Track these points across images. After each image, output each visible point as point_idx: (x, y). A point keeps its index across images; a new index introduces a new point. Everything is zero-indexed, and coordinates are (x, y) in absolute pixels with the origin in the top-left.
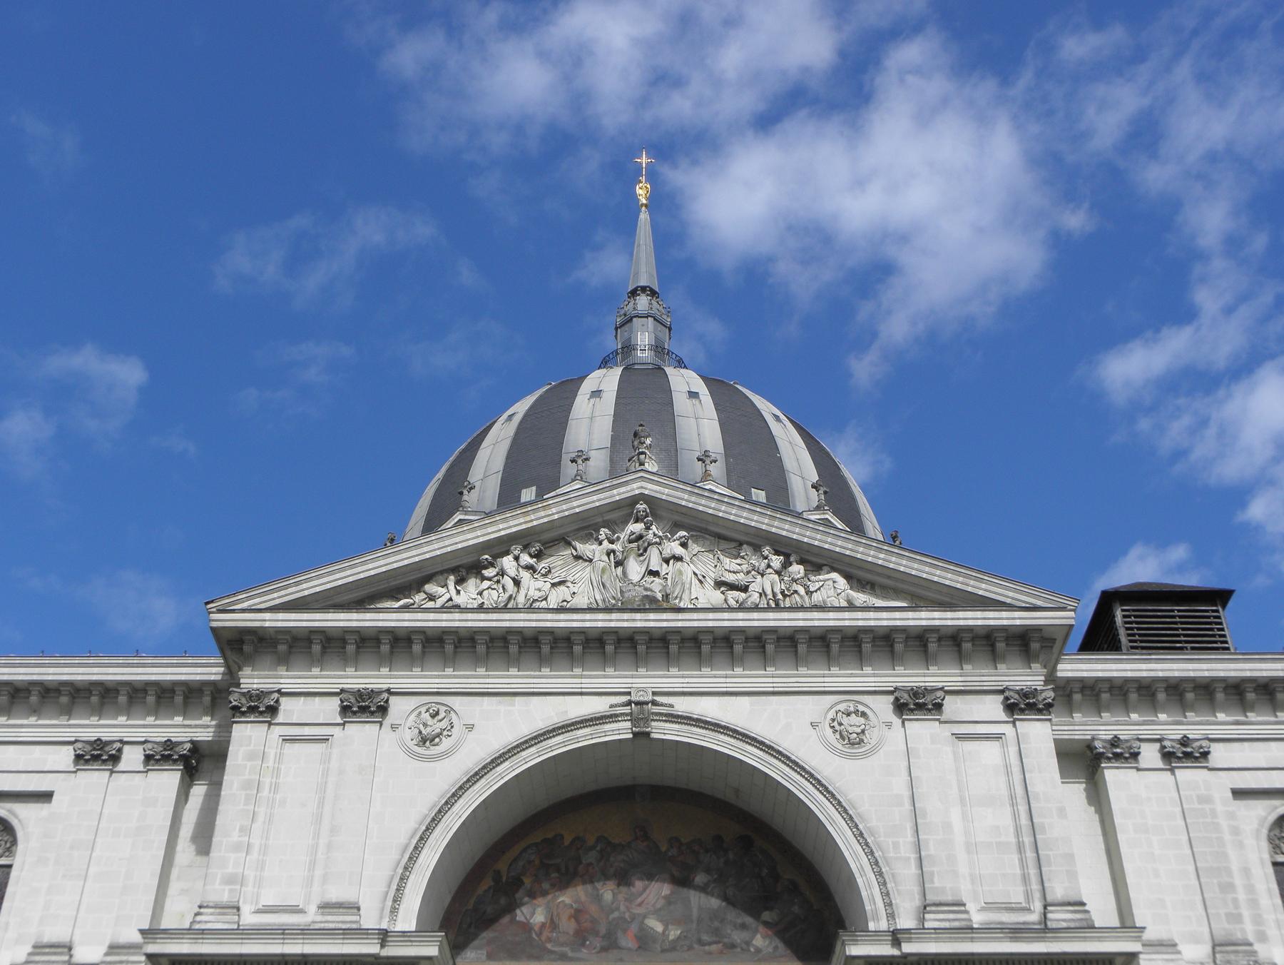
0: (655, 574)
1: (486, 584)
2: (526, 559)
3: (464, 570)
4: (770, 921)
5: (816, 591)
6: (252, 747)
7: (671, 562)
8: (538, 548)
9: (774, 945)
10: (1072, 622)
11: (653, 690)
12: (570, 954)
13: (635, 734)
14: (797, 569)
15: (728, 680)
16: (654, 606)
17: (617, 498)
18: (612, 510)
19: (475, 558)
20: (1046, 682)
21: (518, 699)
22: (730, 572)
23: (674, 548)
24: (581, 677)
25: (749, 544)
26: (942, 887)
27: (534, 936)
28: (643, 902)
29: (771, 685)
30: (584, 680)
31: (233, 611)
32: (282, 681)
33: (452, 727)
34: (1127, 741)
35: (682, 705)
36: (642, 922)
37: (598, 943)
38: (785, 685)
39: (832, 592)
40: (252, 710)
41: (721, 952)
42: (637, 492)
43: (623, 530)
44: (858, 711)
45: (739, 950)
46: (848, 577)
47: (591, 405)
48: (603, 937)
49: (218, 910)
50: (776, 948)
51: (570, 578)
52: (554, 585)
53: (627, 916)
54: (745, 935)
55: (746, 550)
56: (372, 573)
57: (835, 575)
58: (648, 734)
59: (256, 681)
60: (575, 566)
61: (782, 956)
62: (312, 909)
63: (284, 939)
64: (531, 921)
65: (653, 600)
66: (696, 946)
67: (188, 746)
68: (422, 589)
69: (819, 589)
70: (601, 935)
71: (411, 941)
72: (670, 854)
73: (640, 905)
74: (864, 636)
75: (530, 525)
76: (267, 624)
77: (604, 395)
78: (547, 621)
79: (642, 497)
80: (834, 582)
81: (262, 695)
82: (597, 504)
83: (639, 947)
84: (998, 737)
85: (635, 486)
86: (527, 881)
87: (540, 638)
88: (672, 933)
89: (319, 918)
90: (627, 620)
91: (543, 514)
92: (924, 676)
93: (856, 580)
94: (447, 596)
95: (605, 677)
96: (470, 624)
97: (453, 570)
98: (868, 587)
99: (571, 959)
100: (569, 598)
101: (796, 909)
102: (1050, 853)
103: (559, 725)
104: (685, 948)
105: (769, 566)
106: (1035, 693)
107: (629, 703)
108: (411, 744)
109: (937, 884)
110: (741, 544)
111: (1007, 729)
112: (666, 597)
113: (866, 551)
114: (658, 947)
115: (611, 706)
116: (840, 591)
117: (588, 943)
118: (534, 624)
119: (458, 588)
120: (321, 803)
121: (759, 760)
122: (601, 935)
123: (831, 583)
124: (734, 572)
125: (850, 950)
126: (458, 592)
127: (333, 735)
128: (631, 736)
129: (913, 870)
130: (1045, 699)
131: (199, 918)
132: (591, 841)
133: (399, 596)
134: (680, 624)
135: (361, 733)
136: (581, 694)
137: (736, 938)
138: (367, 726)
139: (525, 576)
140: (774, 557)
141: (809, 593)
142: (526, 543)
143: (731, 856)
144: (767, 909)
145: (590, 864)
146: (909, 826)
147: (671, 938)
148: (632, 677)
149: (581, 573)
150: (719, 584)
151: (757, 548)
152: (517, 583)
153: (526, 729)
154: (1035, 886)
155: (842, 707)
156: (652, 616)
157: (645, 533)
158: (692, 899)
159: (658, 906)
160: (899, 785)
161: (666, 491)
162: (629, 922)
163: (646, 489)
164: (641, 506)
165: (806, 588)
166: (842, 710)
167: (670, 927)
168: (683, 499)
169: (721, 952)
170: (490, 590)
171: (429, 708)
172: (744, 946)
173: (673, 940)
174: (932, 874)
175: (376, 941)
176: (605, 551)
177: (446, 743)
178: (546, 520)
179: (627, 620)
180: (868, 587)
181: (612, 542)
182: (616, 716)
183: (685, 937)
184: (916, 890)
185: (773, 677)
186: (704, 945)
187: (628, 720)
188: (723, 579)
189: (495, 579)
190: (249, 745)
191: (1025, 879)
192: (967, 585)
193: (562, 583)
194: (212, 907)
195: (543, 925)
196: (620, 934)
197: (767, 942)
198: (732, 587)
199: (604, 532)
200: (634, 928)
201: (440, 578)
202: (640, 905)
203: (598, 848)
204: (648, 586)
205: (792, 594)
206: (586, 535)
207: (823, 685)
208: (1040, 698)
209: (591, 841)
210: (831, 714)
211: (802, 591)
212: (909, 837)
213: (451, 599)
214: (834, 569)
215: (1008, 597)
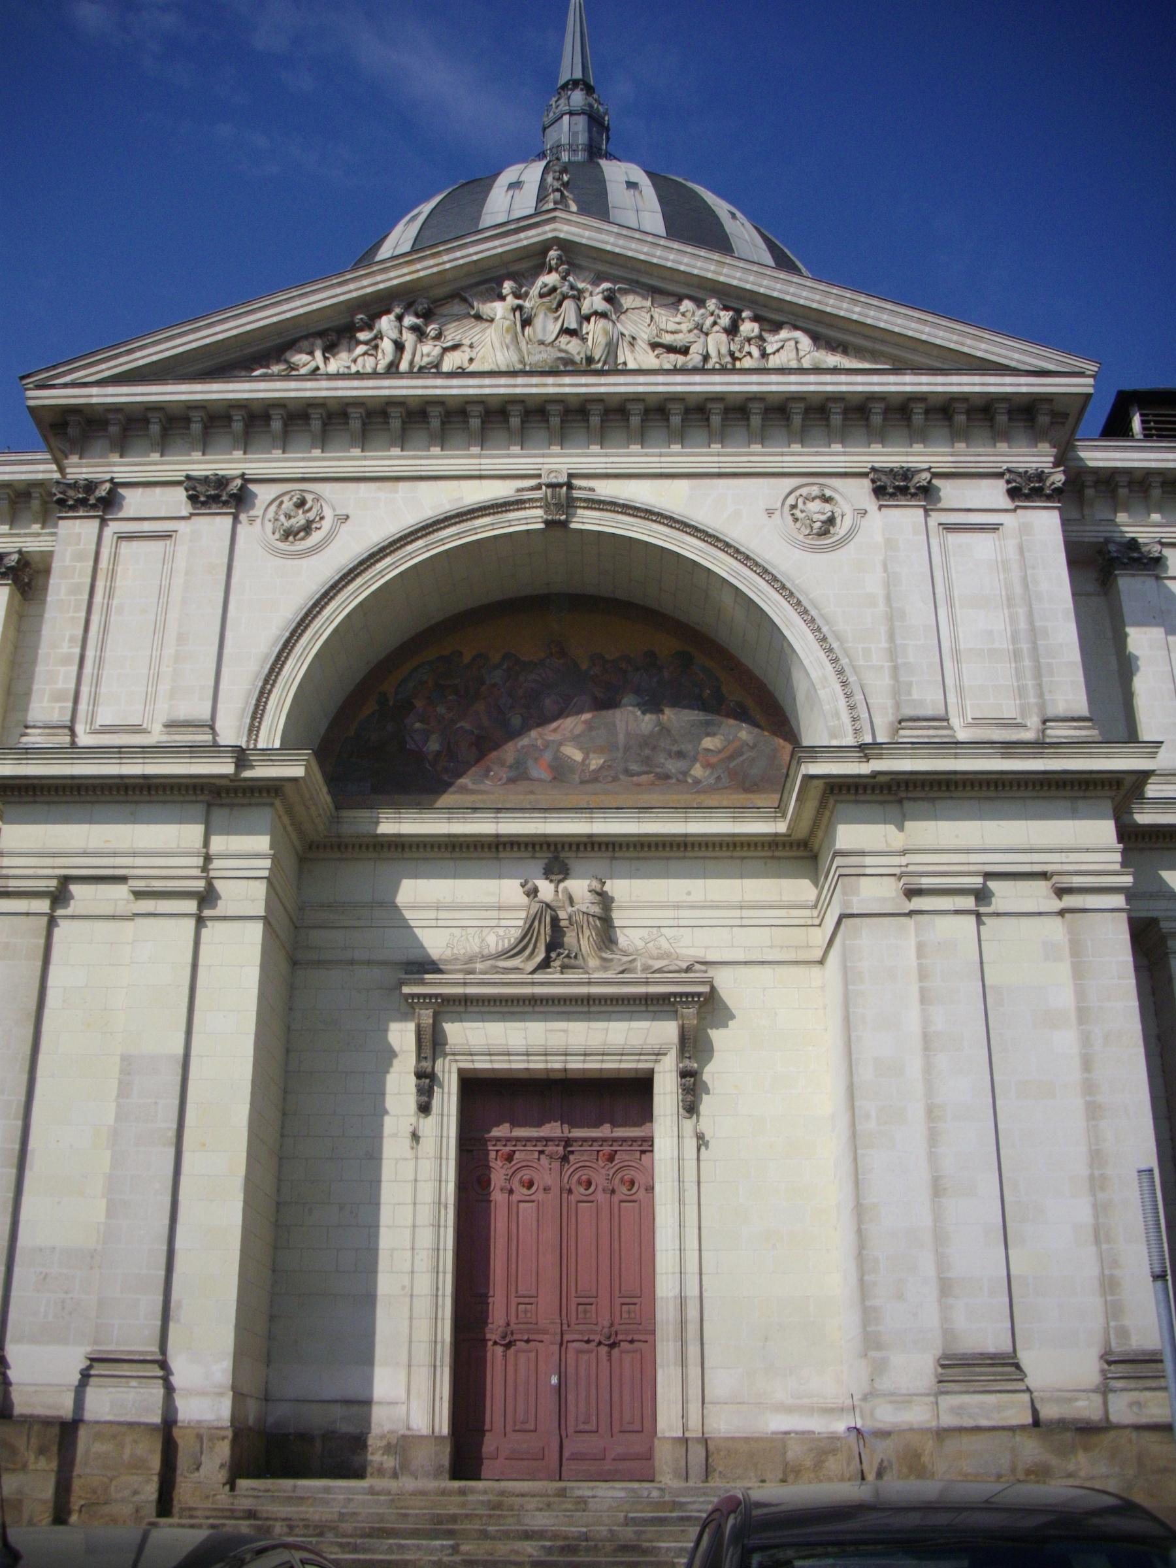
1: (361, 349)
3: (334, 334)
4: (712, 748)
5: (774, 353)
6: (81, 547)
7: (593, 319)
8: (426, 306)
9: (716, 775)
10: (1091, 390)
11: (570, 471)
12: (471, 786)
13: (548, 523)
14: (749, 328)
15: (663, 459)
16: (569, 368)
17: (525, 243)
18: (520, 259)
19: (349, 320)
20: (1056, 464)
21: (402, 485)
22: (667, 332)
24: (480, 456)
25: (691, 298)
27: (427, 765)
28: (558, 727)
29: (717, 465)
30: (483, 461)
31: (53, 387)
32: (116, 469)
33: (322, 518)
34: (1146, 544)
35: (605, 489)
36: (558, 750)
37: (504, 774)
38: (734, 465)
39: (793, 355)
40: (83, 502)
41: (652, 784)
42: (550, 235)
43: (533, 284)
44: (824, 495)
45: (674, 781)
48: (510, 767)
49: (47, 731)
50: (719, 778)
51: (467, 342)
52: (445, 350)
53: (539, 742)
54: (681, 765)
55: (687, 305)
56: (220, 337)
57: (798, 334)
58: (564, 524)
59: (84, 470)
60: (473, 327)
61: (726, 788)
63: (120, 758)
64: (425, 749)
65: (569, 361)
66: (622, 777)
67: (15, 557)
68: (283, 358)
69: (778, 350)
70: (508, 764)
71: (272, 760)
72: (592, 673)
73: (555, 731)
74: (834, 405)
75: (415, 276)
76: (94, 400)
77: (526, 187)
78: (436, 387)
80: (797, 343)
81: (91, 486)
82: (500, 250)
83: (554, 778)
84: (994, 528)
85: (547, 228)
86: (419, 704)
87: (429, 409)
88: (594, 762)
89: (164, 738)
90: (536, 385)
91: (431, 262)
92: (907, 455)
93: (824, 343)
94: (313, 365)
95: (509, 456)
96: (340, 393)
97: (320, 334)
98: (840, 349)
99: (472, 792)
100: (466, 364)
102: (1053, 661)
103: (452, 513)
104: (610, 779)
105: (715, 323)
106: (1040, 476)
107: (538, 487)
108: (273, 539)
109: (915, 695)
110: (680, 300)
113: (838, 303)
114: (577, 778)
115: (518, 490)
116: (801, 353)
117: (492, 773)
118: (420, 392)
119: (327, 355)
121: (699, 553)
122: (508, 764)
123: (792, 343)
124: (672, 333)
125: (807, 769)
126: (326, 359)
127: (176, 531)
128: (542, 526)
129: (886, 681)
130: (1053, 483)
132: (496, 658)
133: (255, 367)
134: (602, 390)
136: (480, 477)
137: (670, 767)
138: (218, 519)
139: (409, 338)
140: (722, 313)
141: (764, 355)
142: (411, 300)
143: (666, 675)
144: (708, 735)
145: (495, 685)
146: (883, 630)
147: (592, 767)
148: (543, 456)
150: (654, 346)
151: (700, 303)
152: (399, 347)
153: (410, 519)
154: (1033, 700)
155: (804, 491)
156: (567, 380)
157: (558, 285)
158: (618, 722)
159: (577, 731)
160: (874, 583)
161: (587, 233)
162: (541, 750)
163: (561, 231)
164: (553, 254)
166: (804, 495)
167: (591, 756)
168: (607, 243)
169: (652, 784)
170: (366, 357)
171: (293, 496)
172: (681, 777)
173: (593, 771)
174: (910, 684)
175: (230, 760)
176: (510, 307)
177: (315, 537)
178: (435, 270)
179: (536, 385)
180: (840, 349)
182: (523, 502)
183: (609, 766)
184: (890, 703)
185: (719, 455)
186: (632, 775)
187: (540, 507)
188: (657, 340)
189: (373, 343)
190: (78, 544)
191: (1021, 692)
192: (963, 345)
193: (455, 347)
194: (40, 727)
195: (438, 754)
196: (530, 763)
197: (707, 773)
198: (671, 349)
200: (548, 756)
201: (305, 344)
202: (555, 731)
203: (505, 667)
204: (563, 346)
205: (745, 356)
206: (487, 290)
207: (780, 465)
208: (1048, 484)
209: (496, 658)
210: (791, 500)
211: (756, 352)
212: (884, 644)
213: (317, 368)
214: (796, 328)
215: (1012, 359)
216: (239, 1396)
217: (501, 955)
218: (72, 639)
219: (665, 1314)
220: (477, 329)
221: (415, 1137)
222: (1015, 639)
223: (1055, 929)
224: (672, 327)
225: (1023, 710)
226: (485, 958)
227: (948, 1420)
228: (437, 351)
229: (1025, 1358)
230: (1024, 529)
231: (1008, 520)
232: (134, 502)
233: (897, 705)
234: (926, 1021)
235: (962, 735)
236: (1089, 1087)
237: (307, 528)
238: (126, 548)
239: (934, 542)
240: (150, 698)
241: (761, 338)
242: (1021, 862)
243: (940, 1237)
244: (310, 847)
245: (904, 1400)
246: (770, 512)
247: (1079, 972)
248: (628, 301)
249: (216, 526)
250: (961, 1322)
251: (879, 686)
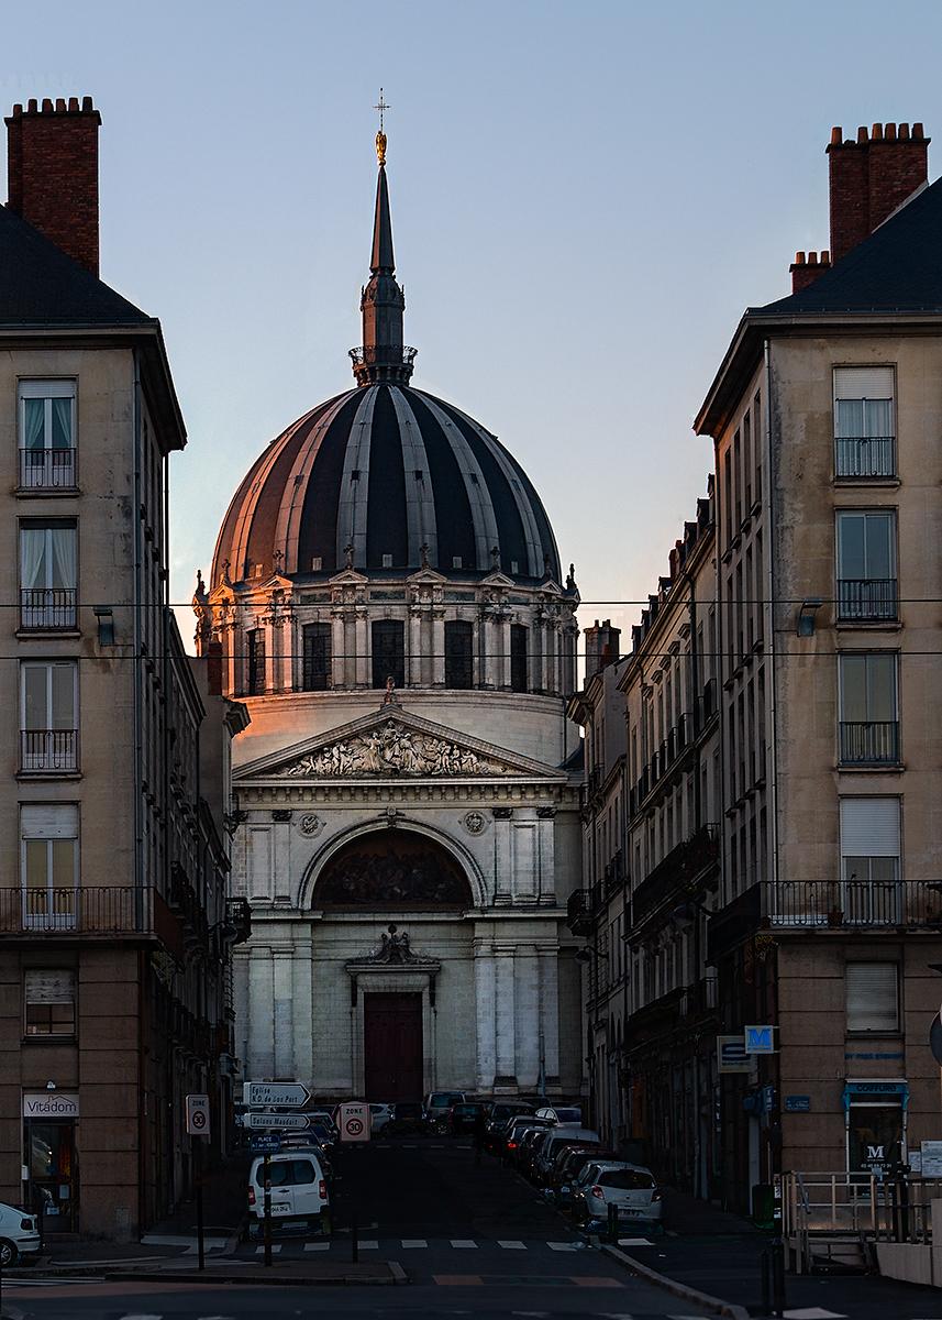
0: (397, 756)
2: (343, 748)
14: (456, 752)
23: (408, 744)
26: (504, 887)
35: (409, 814)
46: (477, 755)
47: (353, 487)
57: (472, 756)
62: (272, 898)
65: (395, 770)
79: (391, 719)
101: (452, 883)
107: (386, 814)
112: (401, 768)
120: (270, 857)
135: (282, 828)
139: (342, 755)
141: (461, 764)
149: (364, 751)
152: (339, 760)
160: (492, 848)
165: (460, 762)
181: (378, 738)
191: (535, 884)
199: (375, 734)
200: (389, 891)
214: (472, 752)
217: (375, 958)
219: (425, 1063)
221: (351, 1013)
222: (534, 866)
223: (535, 961)
225: (534, 891)
226: (371, 958)
227: (496, 1093)
229: (518, 1077)
230: (541, 828)
231: (536, 823)
232: (256, 817)
234: (496, 987)
235: (514, 904)
236: (540, 1007)
237: (314, 828)
241: (461, 756)
242: (529, 941)
243: (496, 1047)
245: (486, 1088)
246: (460, 822)
247: (541, 974)
248: (416, 738)
250: (501, 1069)
251: (491, 883)
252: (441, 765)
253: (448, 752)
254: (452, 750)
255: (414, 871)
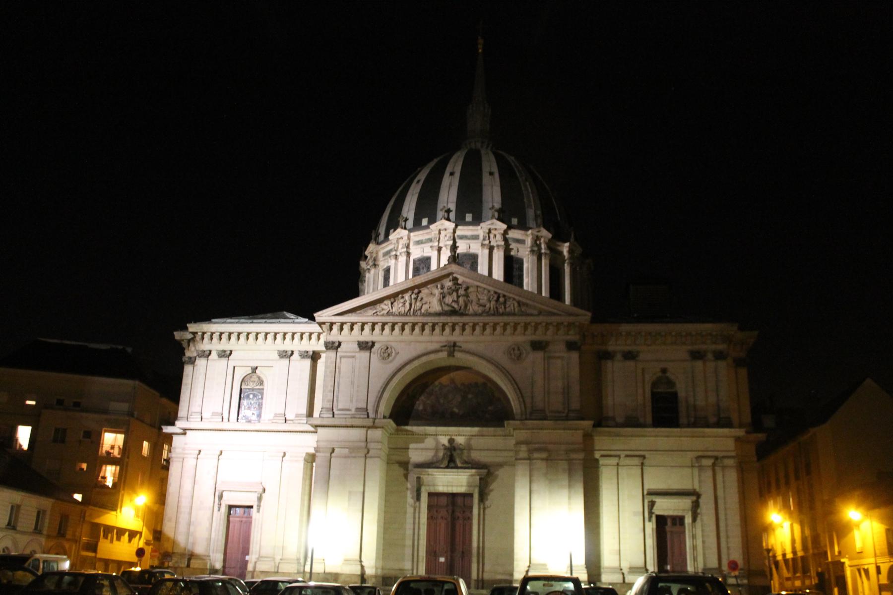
39: (512, 308)
62: (353, 410)
67: (311, 353)
94: (389, 309)
105: (492, 299)
111: (565, 355)
115: (442, 347)
123: (512, 305)
131: (322, 412)
141: (505, 308)
152: (411, 305)
177: (391, 358)
193: (425, 303)
201: (386, 302)
216: (377, 569)
218: (331, 386)
219: (475, 551)
220: (432, 297)
224: (482, 298)
228: (421, 305)
233: (532, 407)
238: (343, 360)
239: (546, 361)
240: (351, 401)
244: (391, 434)
246: (505, 353)
249: (365, 355)
252: (490, 308)
253: (495, 298)
254: (498, 297)
255: (470, 396)
